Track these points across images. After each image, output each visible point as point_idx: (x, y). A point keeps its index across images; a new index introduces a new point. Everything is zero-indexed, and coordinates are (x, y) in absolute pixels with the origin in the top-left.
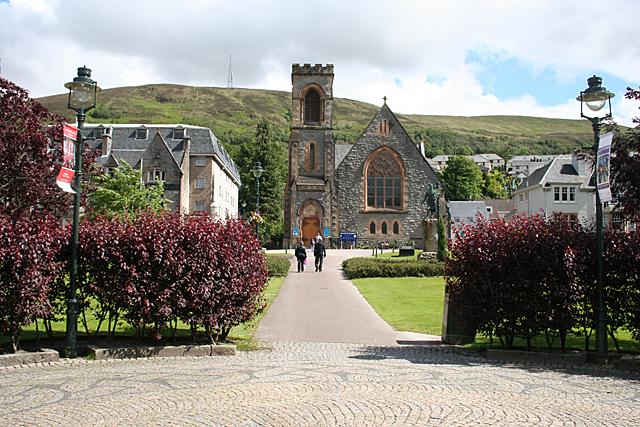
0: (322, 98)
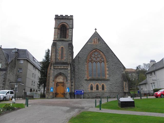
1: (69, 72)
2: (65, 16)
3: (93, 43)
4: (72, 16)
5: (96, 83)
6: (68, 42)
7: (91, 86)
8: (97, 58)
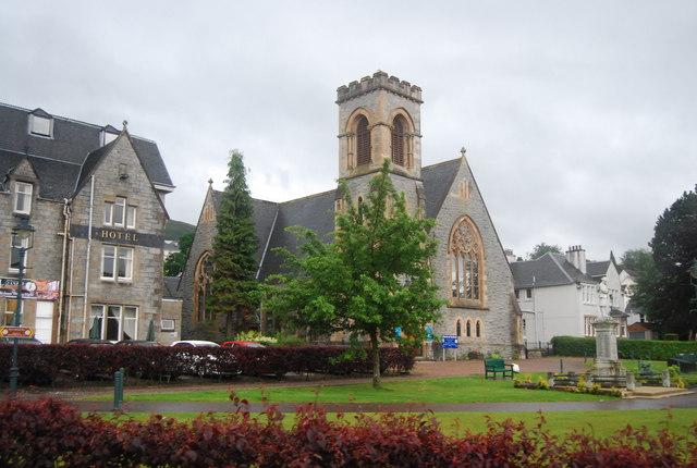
4: (416, 89)
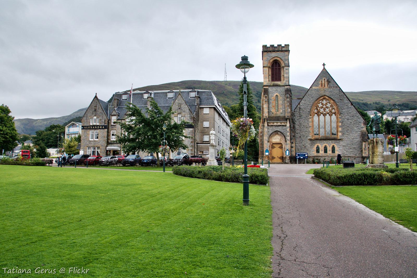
0: (283, 65)
1: (288, 129)
2: (277, 46)
3: (320, 86)
4: (287, 46)
5: (324, 143)
6: (284, 87)
7: (317, 147)
8: (326, 109)
